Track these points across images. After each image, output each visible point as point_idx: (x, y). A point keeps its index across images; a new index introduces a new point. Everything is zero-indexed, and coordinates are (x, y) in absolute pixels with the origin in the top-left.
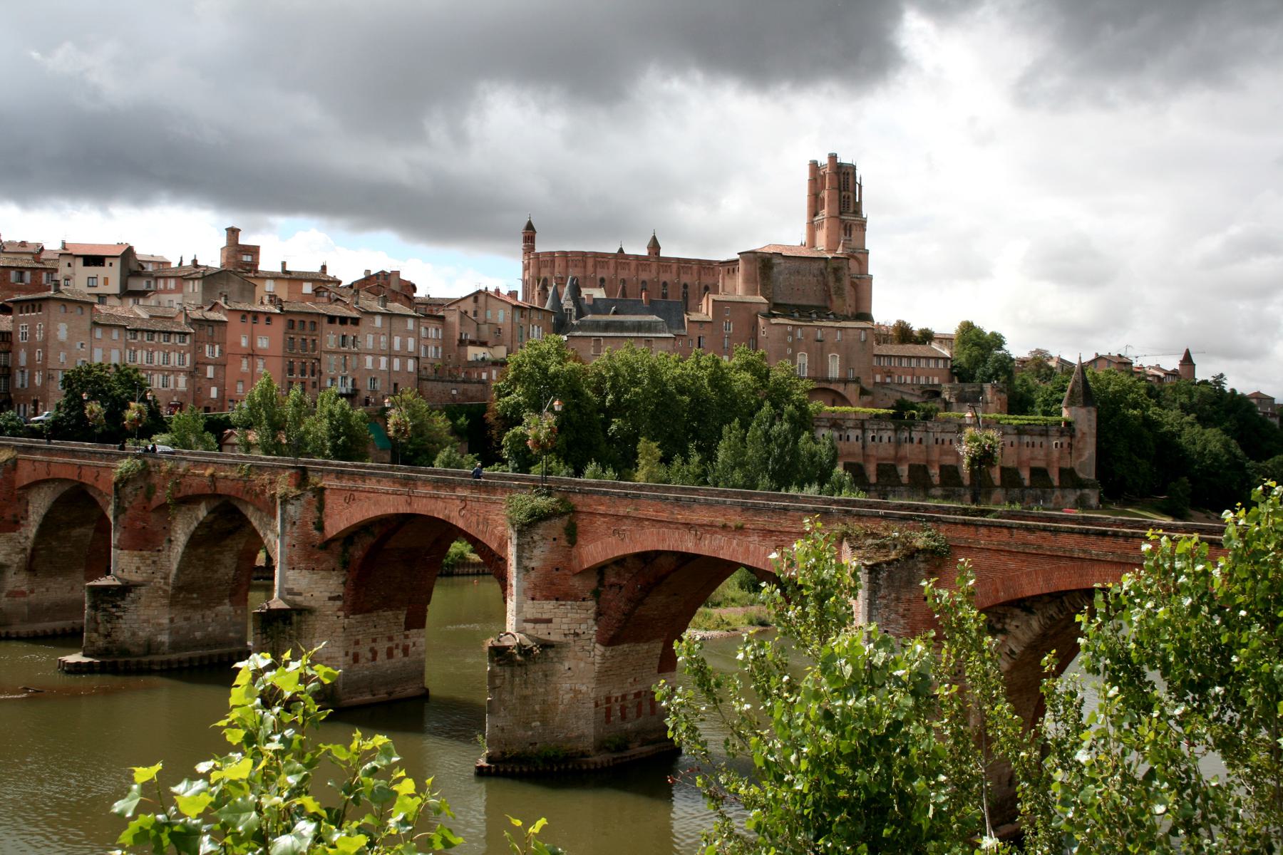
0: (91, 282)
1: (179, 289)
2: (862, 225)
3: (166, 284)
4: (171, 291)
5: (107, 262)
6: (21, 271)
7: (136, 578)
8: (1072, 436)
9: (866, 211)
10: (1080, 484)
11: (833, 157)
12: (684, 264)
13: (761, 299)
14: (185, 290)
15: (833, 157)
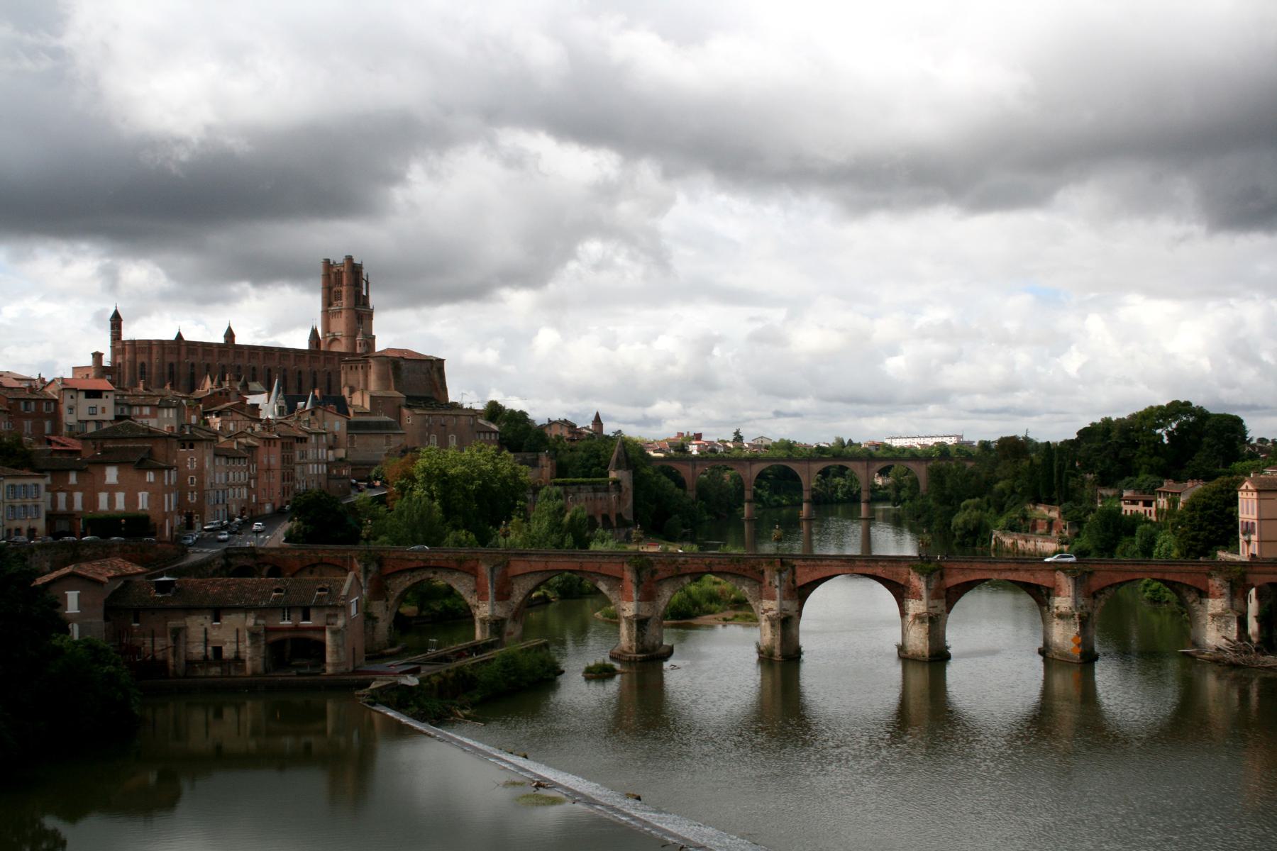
0: (93, 410)
1: (153, 415)
4: (146, 416)
5: (104, 395)
6: (27, 401)
7: (649, 615)
8: (620, 491)
12: (253, 350)
13: (397, 394)
14: (160, 415)
15: (349, 259)
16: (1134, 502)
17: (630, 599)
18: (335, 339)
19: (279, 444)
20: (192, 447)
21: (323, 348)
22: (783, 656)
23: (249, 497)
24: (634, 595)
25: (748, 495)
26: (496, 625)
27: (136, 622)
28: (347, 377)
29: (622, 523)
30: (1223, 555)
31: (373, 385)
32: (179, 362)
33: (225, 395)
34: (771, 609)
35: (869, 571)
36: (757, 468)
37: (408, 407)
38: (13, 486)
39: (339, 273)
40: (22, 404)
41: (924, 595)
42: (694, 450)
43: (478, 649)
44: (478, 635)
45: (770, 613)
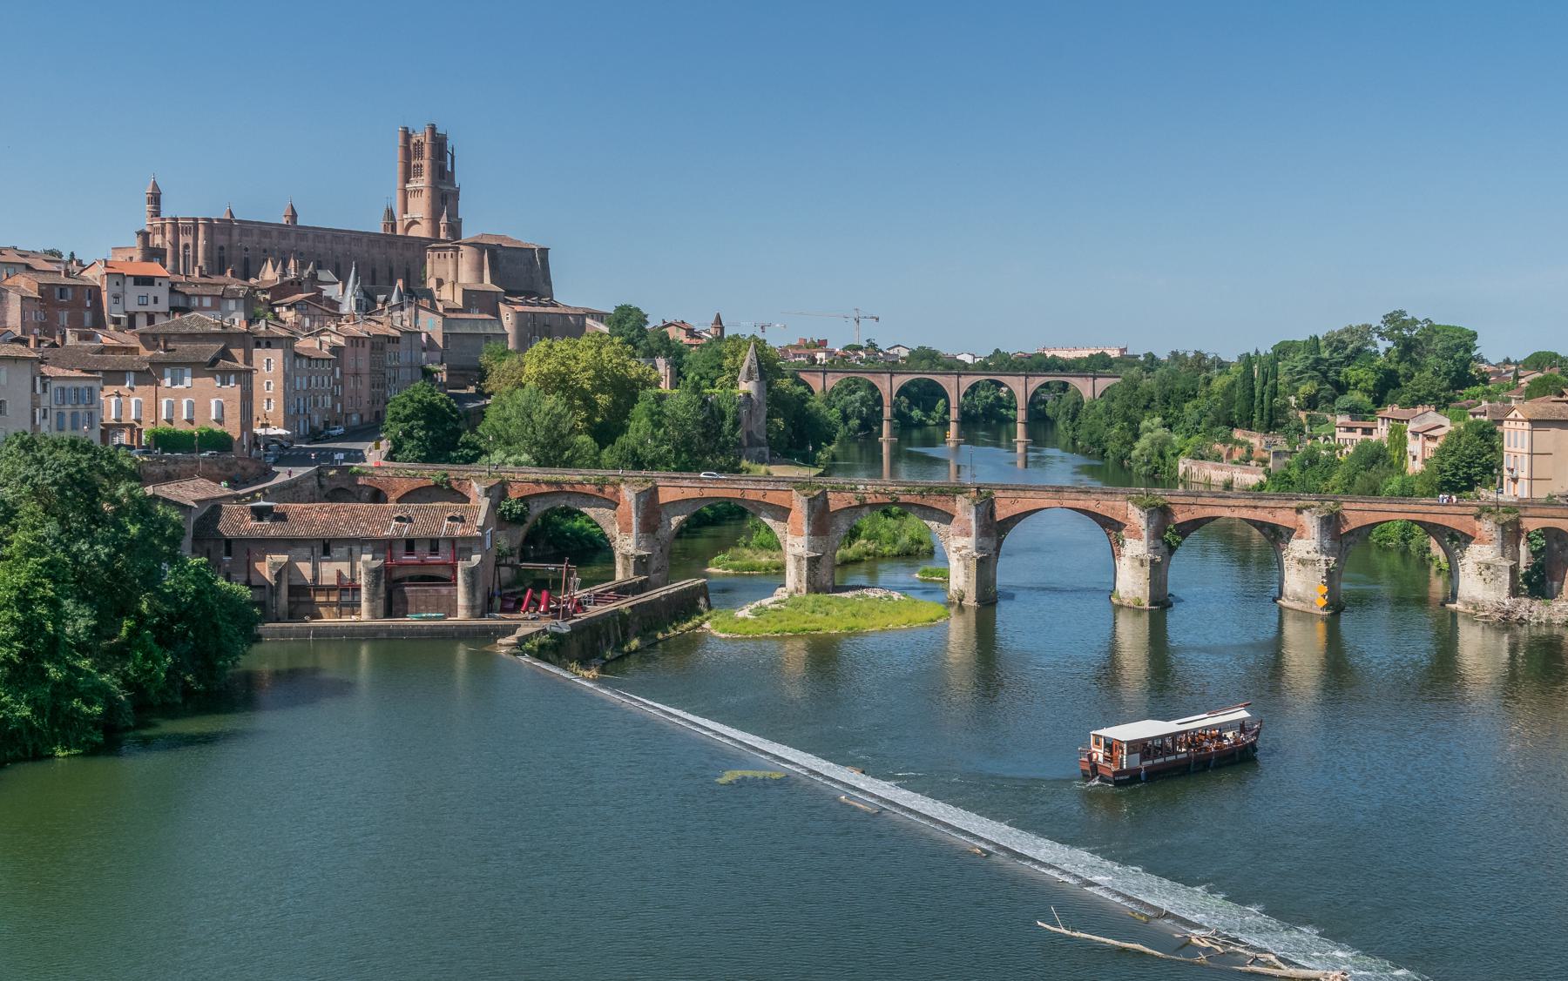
2: (456, 194)
3: (200, 302)
4: (207, 309)
5: (157, 281)
9: (458, 180)
10: (760, 444)
11: (433, 128)
12: (319, 234)
14: (223, 307)
15: (433, 128)
16: (1350, 429)
17: (799, 534)
18: (414, 222)
19: (368, 344)
20: (269, 345)
21: (399, 232)
22: (979, 600)
23: (334, 406)
24: (805, 529)
25: (887, 412)
26: (641, 564)
27: (228, 553)
28: (436, 267)
29: (753, 442)
30: (1487, 494)
31: (466, 277)
32: (230, 246)
33: (296, 286)
34: (965, 547)
35: (1080, 504)
36: (900, 380)
37: (505, 302)
38: (63, 389)
39: (419, 145)
40: (57, 291)
41: (1145, 534)
42: (820, 356)
43: (623, 591)
44: (619, 576)
45: (964, 552)
